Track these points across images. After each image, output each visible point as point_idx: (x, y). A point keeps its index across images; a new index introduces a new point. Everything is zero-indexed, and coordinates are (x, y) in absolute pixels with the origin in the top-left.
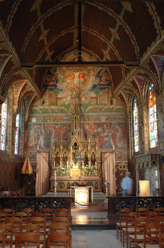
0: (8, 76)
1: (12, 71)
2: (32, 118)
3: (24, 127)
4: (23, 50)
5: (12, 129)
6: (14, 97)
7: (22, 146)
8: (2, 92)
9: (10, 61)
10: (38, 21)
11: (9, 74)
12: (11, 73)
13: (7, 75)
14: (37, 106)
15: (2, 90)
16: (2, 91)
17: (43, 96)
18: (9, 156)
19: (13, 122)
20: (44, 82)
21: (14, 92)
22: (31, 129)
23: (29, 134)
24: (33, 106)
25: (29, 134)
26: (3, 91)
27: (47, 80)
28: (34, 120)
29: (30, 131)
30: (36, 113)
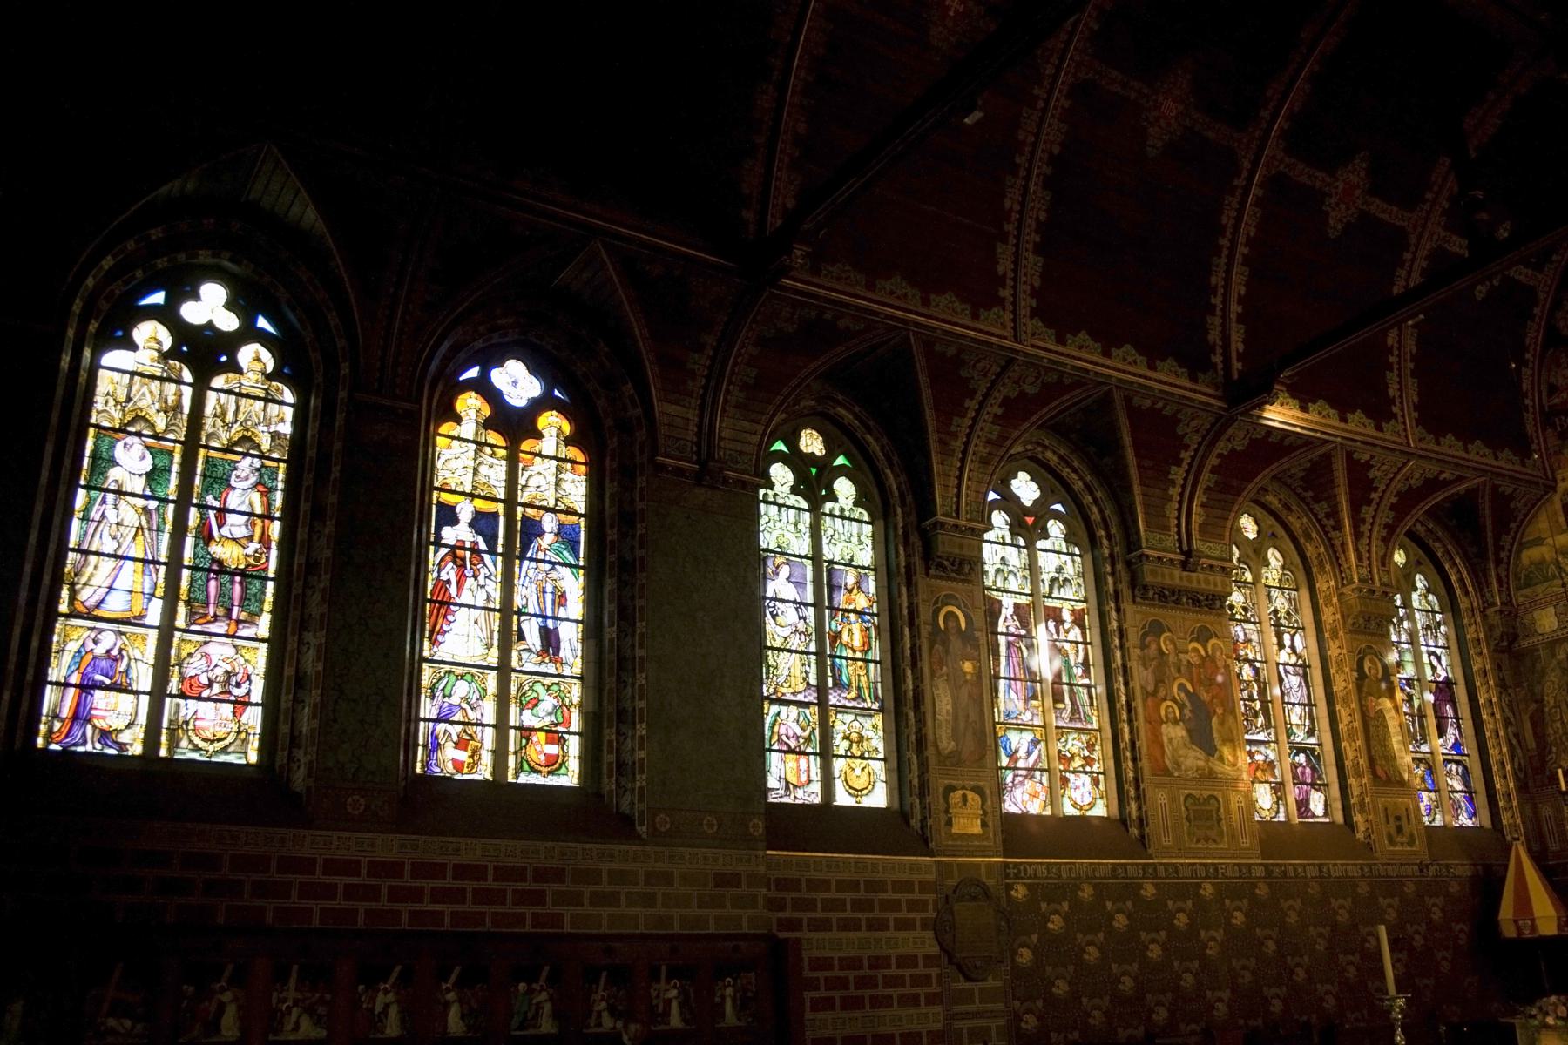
0: (1188, 472)
1: (1200, 444)
2: (1536, 614)
3: (1490, 675)
4: (1223, 325)
5: (1361, 706)
6: (1332, 546)
7: (1505, 777)
8: (1182, 557)
9: (1134, 413)
10: (1246, 164)
11: (1190, 465)
12: (1200, 453)
13: (1177, 473)
14: (1539, 542)
15: (1180, 548)
16: (1182, 552)
17: (1559, 477)
18: (1369, 846)
19: (1360, 667)
20: (1544, 394)
21: (1325, 521)
22: (1543, 673)
23: (1536, 702)
24: (1523, 546)
25: (1540, 701)
26: (1185, 548)
27: (1552, 380)
28: (1547, 621)
29: (1537, 689)
30: (1546, 579)
